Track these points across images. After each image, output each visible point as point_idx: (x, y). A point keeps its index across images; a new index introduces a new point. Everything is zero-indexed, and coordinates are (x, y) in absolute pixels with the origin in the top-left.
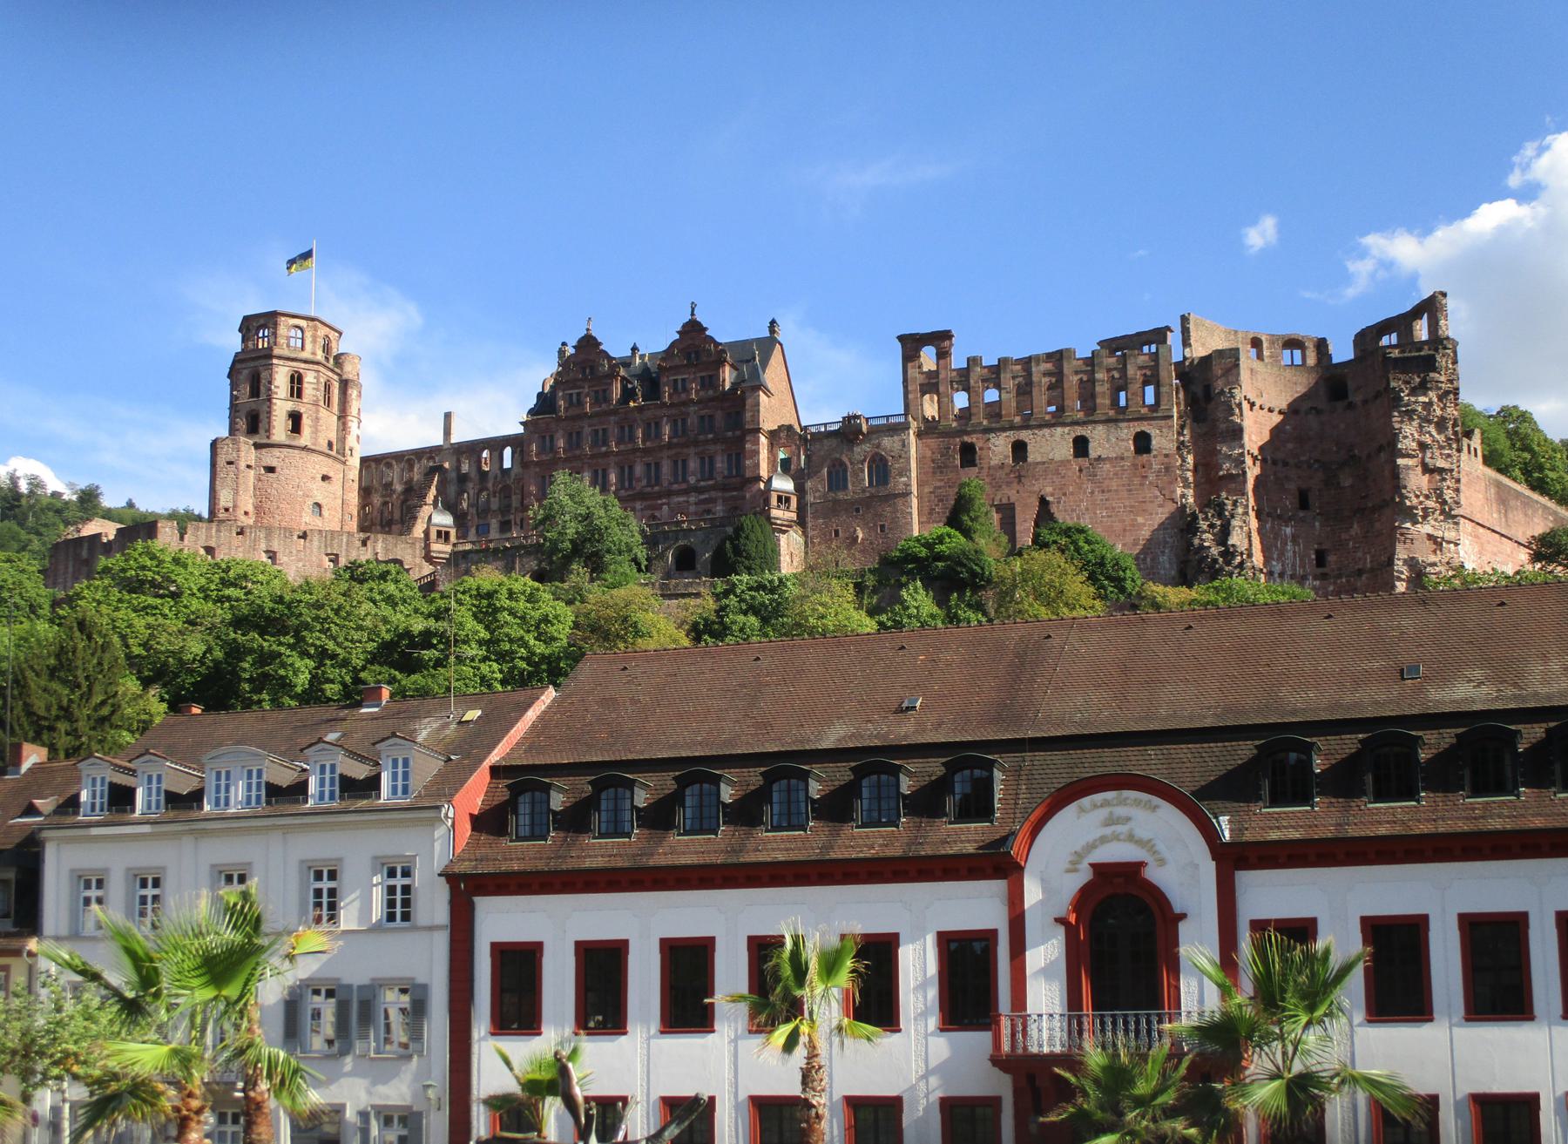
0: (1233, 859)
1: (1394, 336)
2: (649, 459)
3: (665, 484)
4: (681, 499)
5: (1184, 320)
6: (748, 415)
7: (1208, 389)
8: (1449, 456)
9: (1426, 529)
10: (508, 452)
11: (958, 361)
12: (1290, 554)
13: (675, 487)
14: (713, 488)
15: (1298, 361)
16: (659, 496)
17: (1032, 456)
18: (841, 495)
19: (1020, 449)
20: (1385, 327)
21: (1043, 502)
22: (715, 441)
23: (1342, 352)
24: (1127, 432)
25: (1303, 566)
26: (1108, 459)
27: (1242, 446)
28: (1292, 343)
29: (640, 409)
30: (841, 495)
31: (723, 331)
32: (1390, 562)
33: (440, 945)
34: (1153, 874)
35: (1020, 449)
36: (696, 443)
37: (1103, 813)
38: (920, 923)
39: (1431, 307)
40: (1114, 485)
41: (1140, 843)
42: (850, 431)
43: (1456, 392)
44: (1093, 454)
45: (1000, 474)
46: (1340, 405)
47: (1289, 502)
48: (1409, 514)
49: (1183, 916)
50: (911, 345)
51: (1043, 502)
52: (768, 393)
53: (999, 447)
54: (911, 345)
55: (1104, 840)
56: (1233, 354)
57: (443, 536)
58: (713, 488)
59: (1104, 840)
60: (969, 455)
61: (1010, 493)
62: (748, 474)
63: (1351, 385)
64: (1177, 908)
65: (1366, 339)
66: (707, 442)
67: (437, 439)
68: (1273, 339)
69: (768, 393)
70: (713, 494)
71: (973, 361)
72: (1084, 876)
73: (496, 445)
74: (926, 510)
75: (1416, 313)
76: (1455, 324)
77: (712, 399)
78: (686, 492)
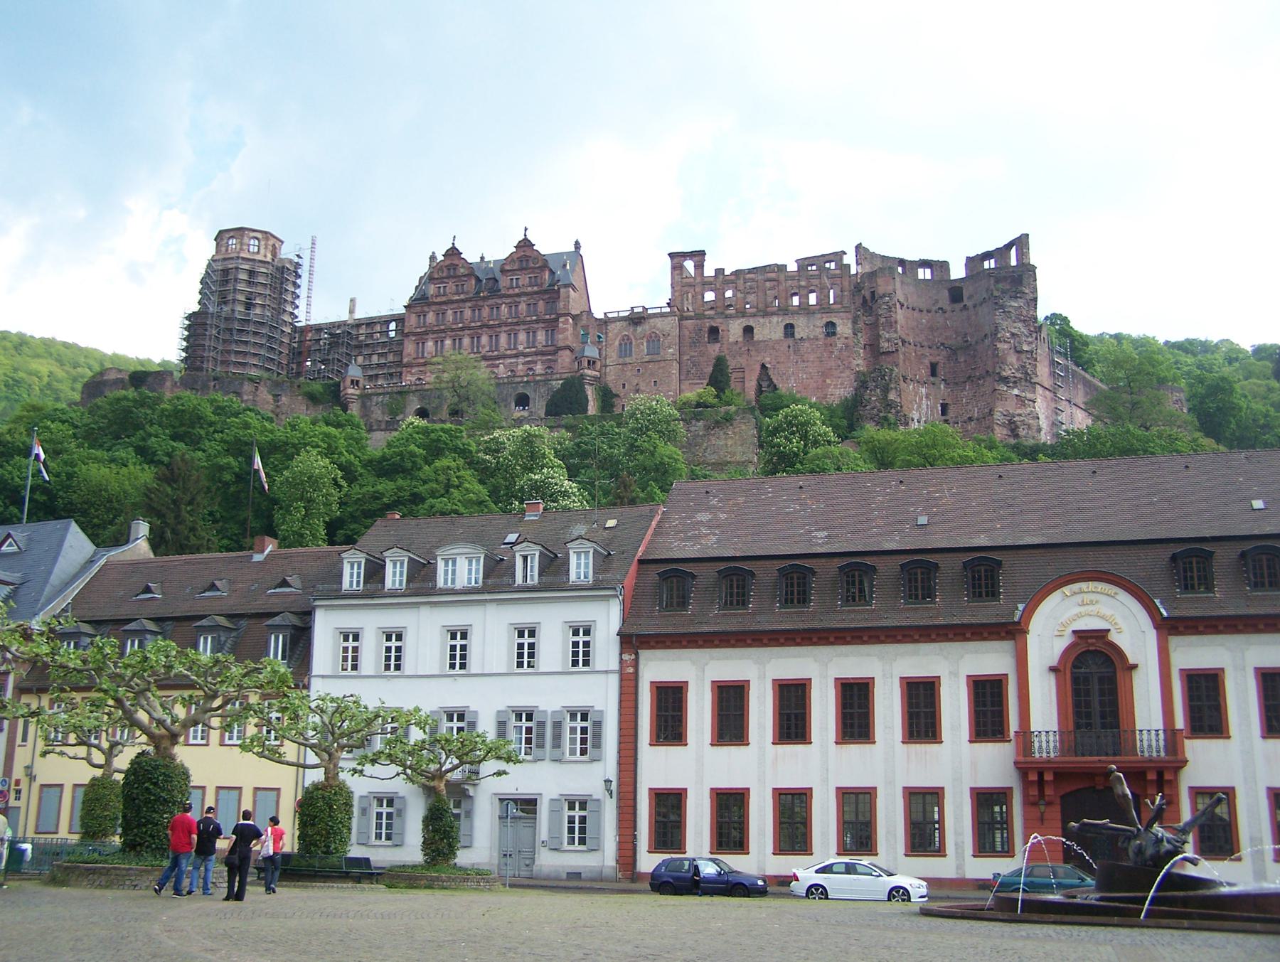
0: (1168, 627)
1: (992, 261)
2: (490, 332)
3: (502, 350)
4: (513, 360)
5: (858, 248)
6: (561, 304)
7: (873, 293)
8: (1030, 343)
9: (1016, 392)
10: (393, 326)
11: (709, 271)
12: (924, 406)
13: (509, 352)
14: (536, 354)
15: (928, 276)
16: (498, 358)
17: (758, 336)
18: (628, 360)
19: (748, 330)
20: (987, 256)
21: (763, 366)
22: (537, 322)
23: (958, 271)
24: (820, 321)
25: (932, 415)
26: (809, 339)
27: (896, 332)
28: (925, 264)
29: (484, 299)
30: (628, 360)
31: (546, 245)
32: (991, 412)
33: (614, 680)
34: (1114, 637)
35: (748, 330)
36: (524, 323)
37: (1078, 598)
38: (954, 668)
39: (1021, 243)
40: (811, 358)
41: (1103, 617)
42: (637, 319)
43: (1035, 300)
44: (797, 336)
45: (735, 347)
46: (958, 306)
47: (924, 372)
48: (1005, 380)
49: (1135, 667)
50: (677, 258)
51: (763, 366)
52: (574, 289)
53: (734, 330)
54: (677, 258)
55: (1080, 616)
56: (892, 270)
57: (355, 383)
58: (536, 354)
59: (1080, 616)
60: (714, 332)
61: (742, 361)
62: (561, 344)
63: (965, 294)
64: (1131, 661)
65: (973, 262)
66: (532, 322)
67: (344, 316)
68: (911, 262)
69: (574, 289)
70: (534, 358)
71: (719, 272)
72: (1067, 640)
73: (386, 321)
74: (684, 372)
75: (1008, 246)
76: (1034, 258)
77: (536, 293)
78: (516, 356)
